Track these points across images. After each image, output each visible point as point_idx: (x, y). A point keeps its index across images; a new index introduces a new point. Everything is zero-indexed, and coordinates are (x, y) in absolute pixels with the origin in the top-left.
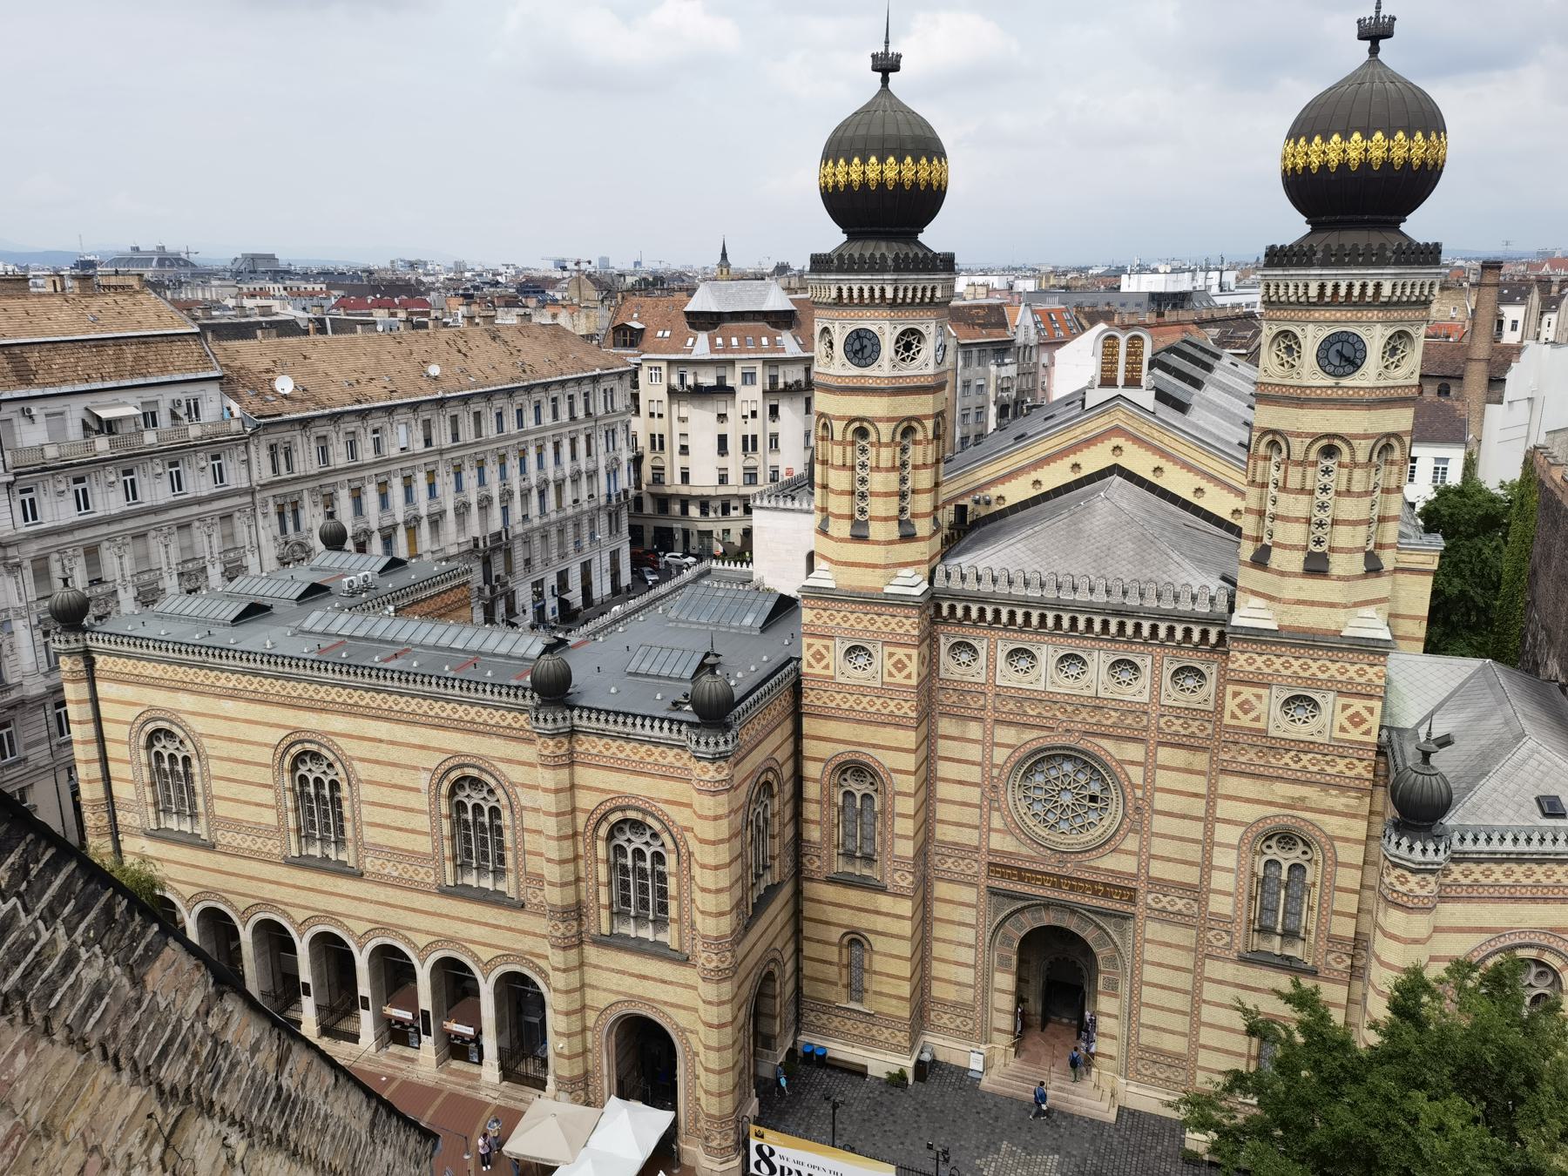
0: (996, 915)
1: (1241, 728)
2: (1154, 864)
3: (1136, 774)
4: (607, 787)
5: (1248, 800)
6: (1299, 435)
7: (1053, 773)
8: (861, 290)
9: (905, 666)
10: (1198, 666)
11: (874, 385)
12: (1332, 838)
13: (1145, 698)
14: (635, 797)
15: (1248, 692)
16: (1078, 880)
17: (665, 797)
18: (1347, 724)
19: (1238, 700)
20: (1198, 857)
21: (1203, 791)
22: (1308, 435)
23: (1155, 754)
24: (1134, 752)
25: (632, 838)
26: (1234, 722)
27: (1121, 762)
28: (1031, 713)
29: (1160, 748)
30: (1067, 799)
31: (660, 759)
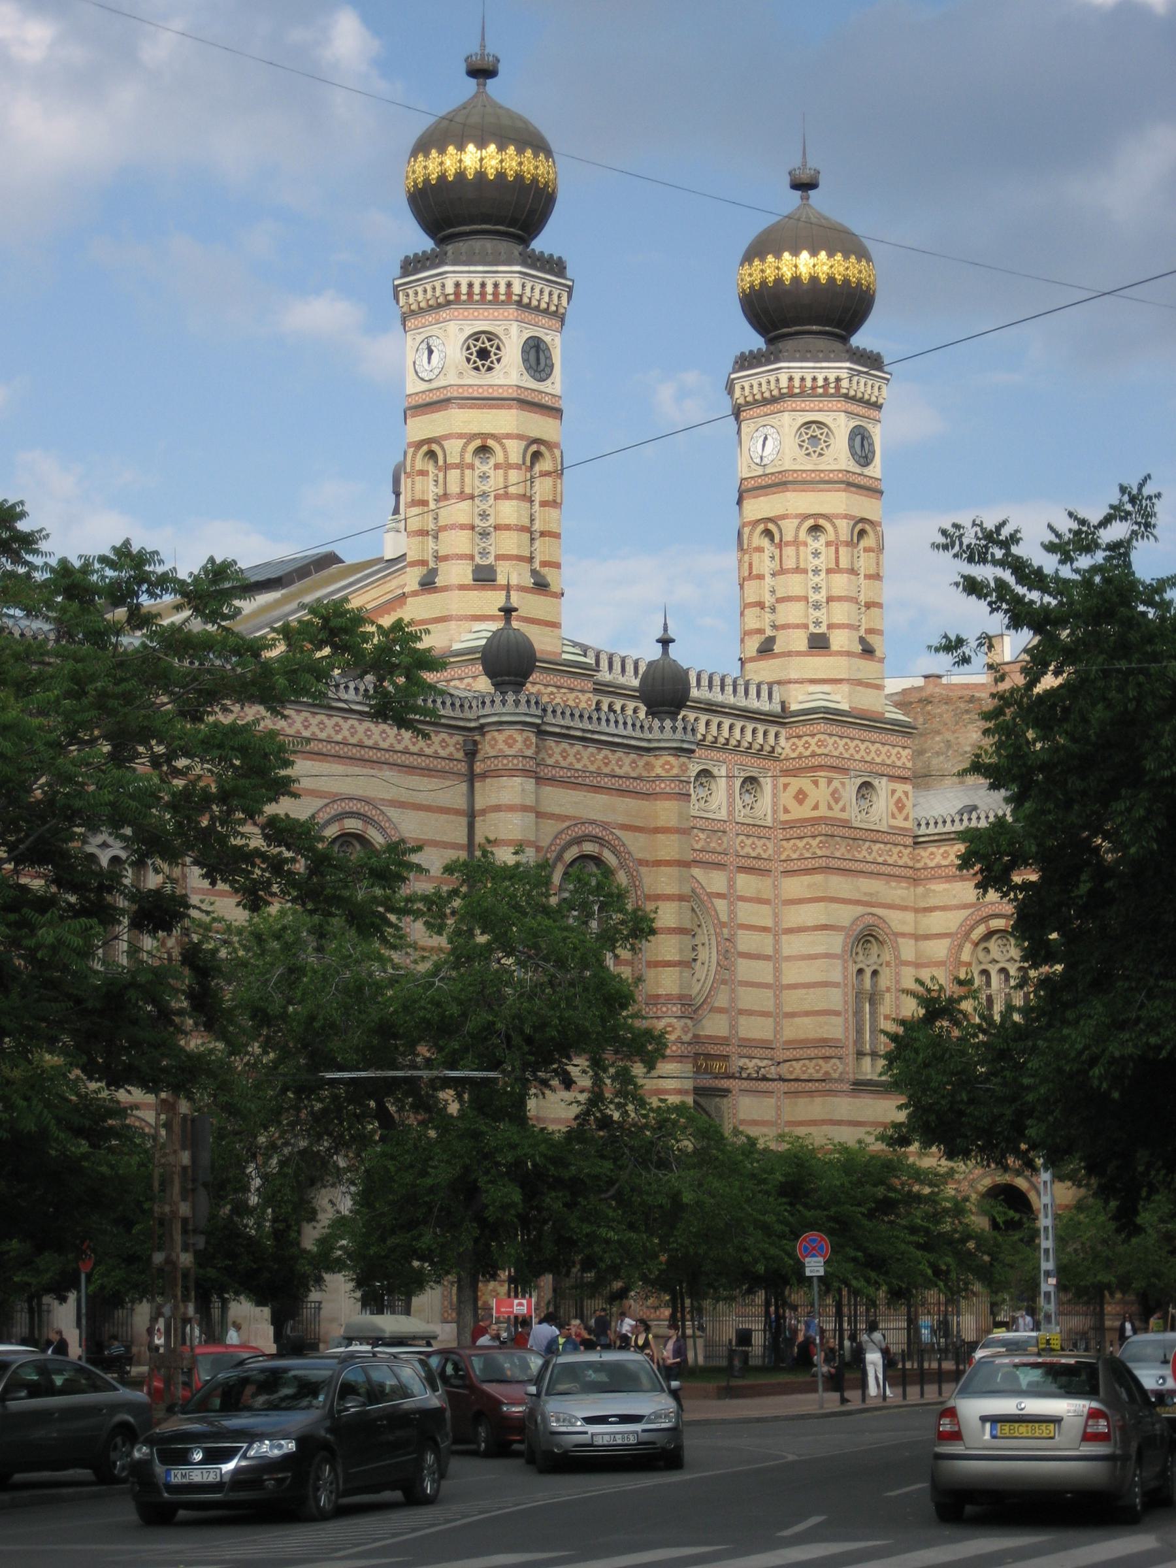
2: (743, 1020)
3: (721, 905)
6: (846, 517)
11: (550, 403)
12: (897, 935)
13: (723, 814)
14: (593, 822)
17: (621, 820)
18: (896, 811)
19: (831, 789)
20: (769, 1006)
21: (769, 923)
24: (716, 881)
26: (829, 814)
27: (712, 895)
31: (617, 769)
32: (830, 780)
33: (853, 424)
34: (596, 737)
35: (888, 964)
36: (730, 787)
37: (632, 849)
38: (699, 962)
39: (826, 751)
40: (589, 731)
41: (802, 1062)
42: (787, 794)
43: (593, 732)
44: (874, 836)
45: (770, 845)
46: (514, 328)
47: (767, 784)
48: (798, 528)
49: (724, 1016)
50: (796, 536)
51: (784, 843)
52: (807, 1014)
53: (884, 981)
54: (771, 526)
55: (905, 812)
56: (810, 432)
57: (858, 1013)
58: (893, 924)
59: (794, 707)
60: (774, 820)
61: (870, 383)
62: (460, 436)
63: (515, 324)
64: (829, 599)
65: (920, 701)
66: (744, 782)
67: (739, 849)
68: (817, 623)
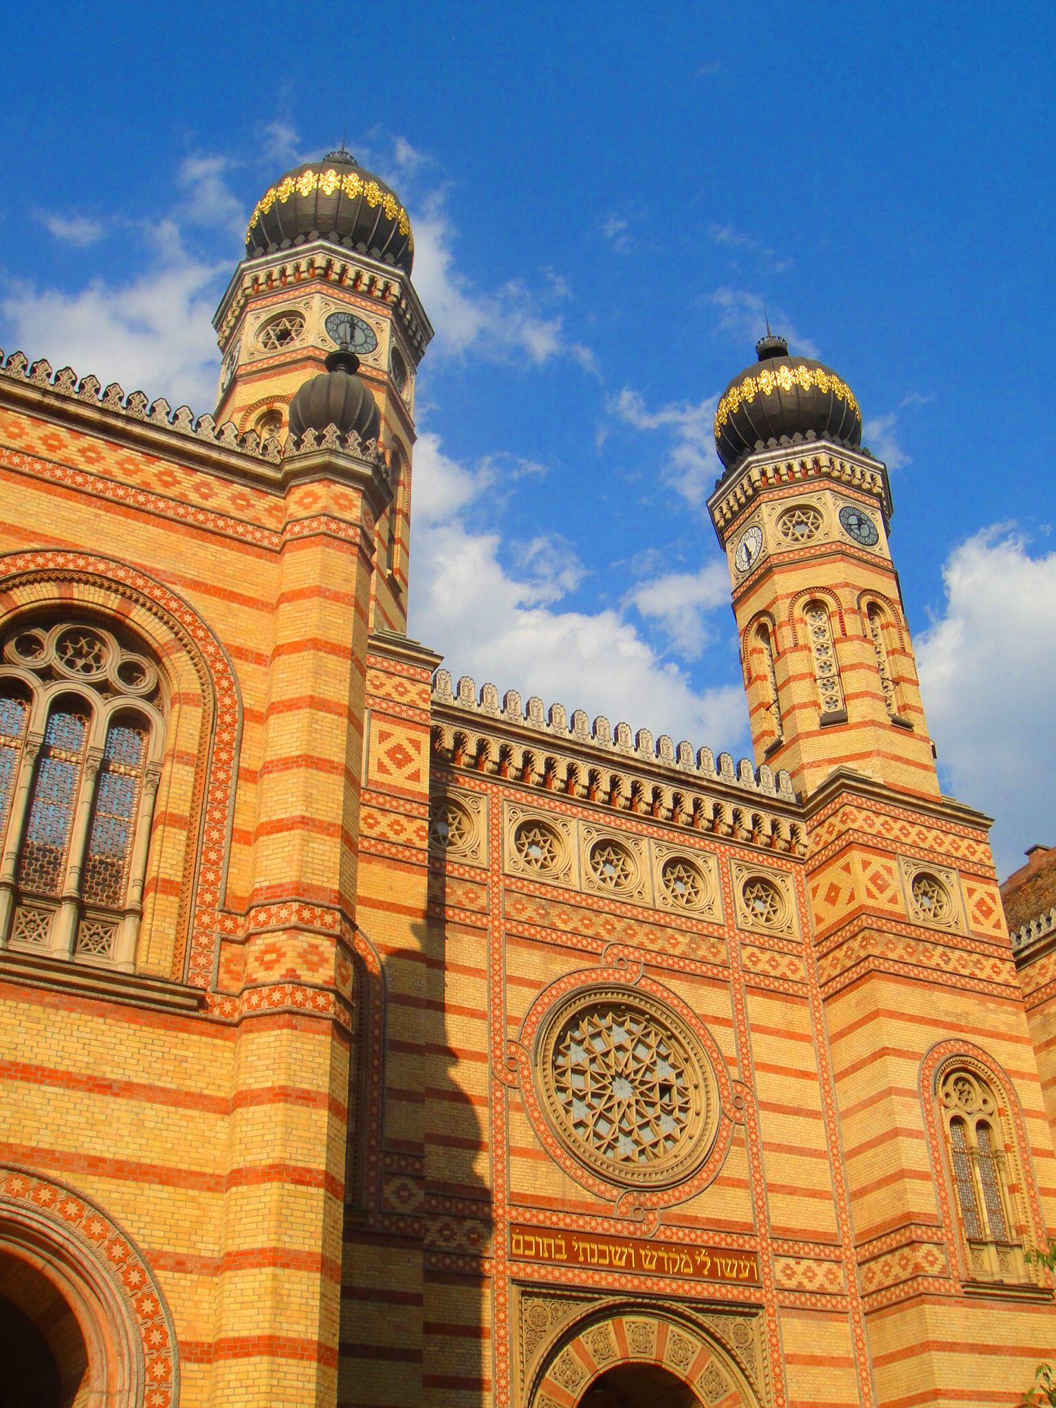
0: (532, 1345)
1: (882, 911)
2: (775, 1200)
3: (725, 1038)
4: (30, 523)
5: (913, 1019)
6: (847, 585)
7: (599, 1046)
8: (358, 276)
9: (408, 759)
10: (771, 878)
12: (1009, 1073)
13: (718, 915)
15: (878, 862)
16: (669, 1245)
17: (191, 574)
19: (870, 871)
22: (854, 587)
23: (745, 1007)
24: (714, 1002)
25: (61, 667)
26: (871, 902)
27: (703, 1019)
28: (562, 926)
29: (749, 998)
30: (623, 1092)
31: (194, 498)
32: (866, 864)
33: (841, 504)
34: (137, 430)
35: (1001, 1112)
36: (726, 885)
37: (218, 627)
38: (691, 1113)
39: (855, 826)
40: (117, 415)
41: (881, 1260)
42: (818, 898)
43: (129, 420)
44: (951, 940)
45: (802, 966)
46: (317, 301)
47: (788, 887)
48: (792, 605)
49: (740, 1192)
50: (791, 614)
51: (823, 961)
52: (881, 1183)
53: (999, 1137)
54: (764, 619)
55: (993, 918)
56: (794, 520)
57: (963, 1180)
58: (1001, 1060)
59: (810, 794)
60: (805, 935)
61: (858, 470)
62: (241, 409)
63: (317, 296)
64: (841, 671)
65: (1029, 880)
66: (750, 883)
67: (750, 965)
68: (831, 701)
